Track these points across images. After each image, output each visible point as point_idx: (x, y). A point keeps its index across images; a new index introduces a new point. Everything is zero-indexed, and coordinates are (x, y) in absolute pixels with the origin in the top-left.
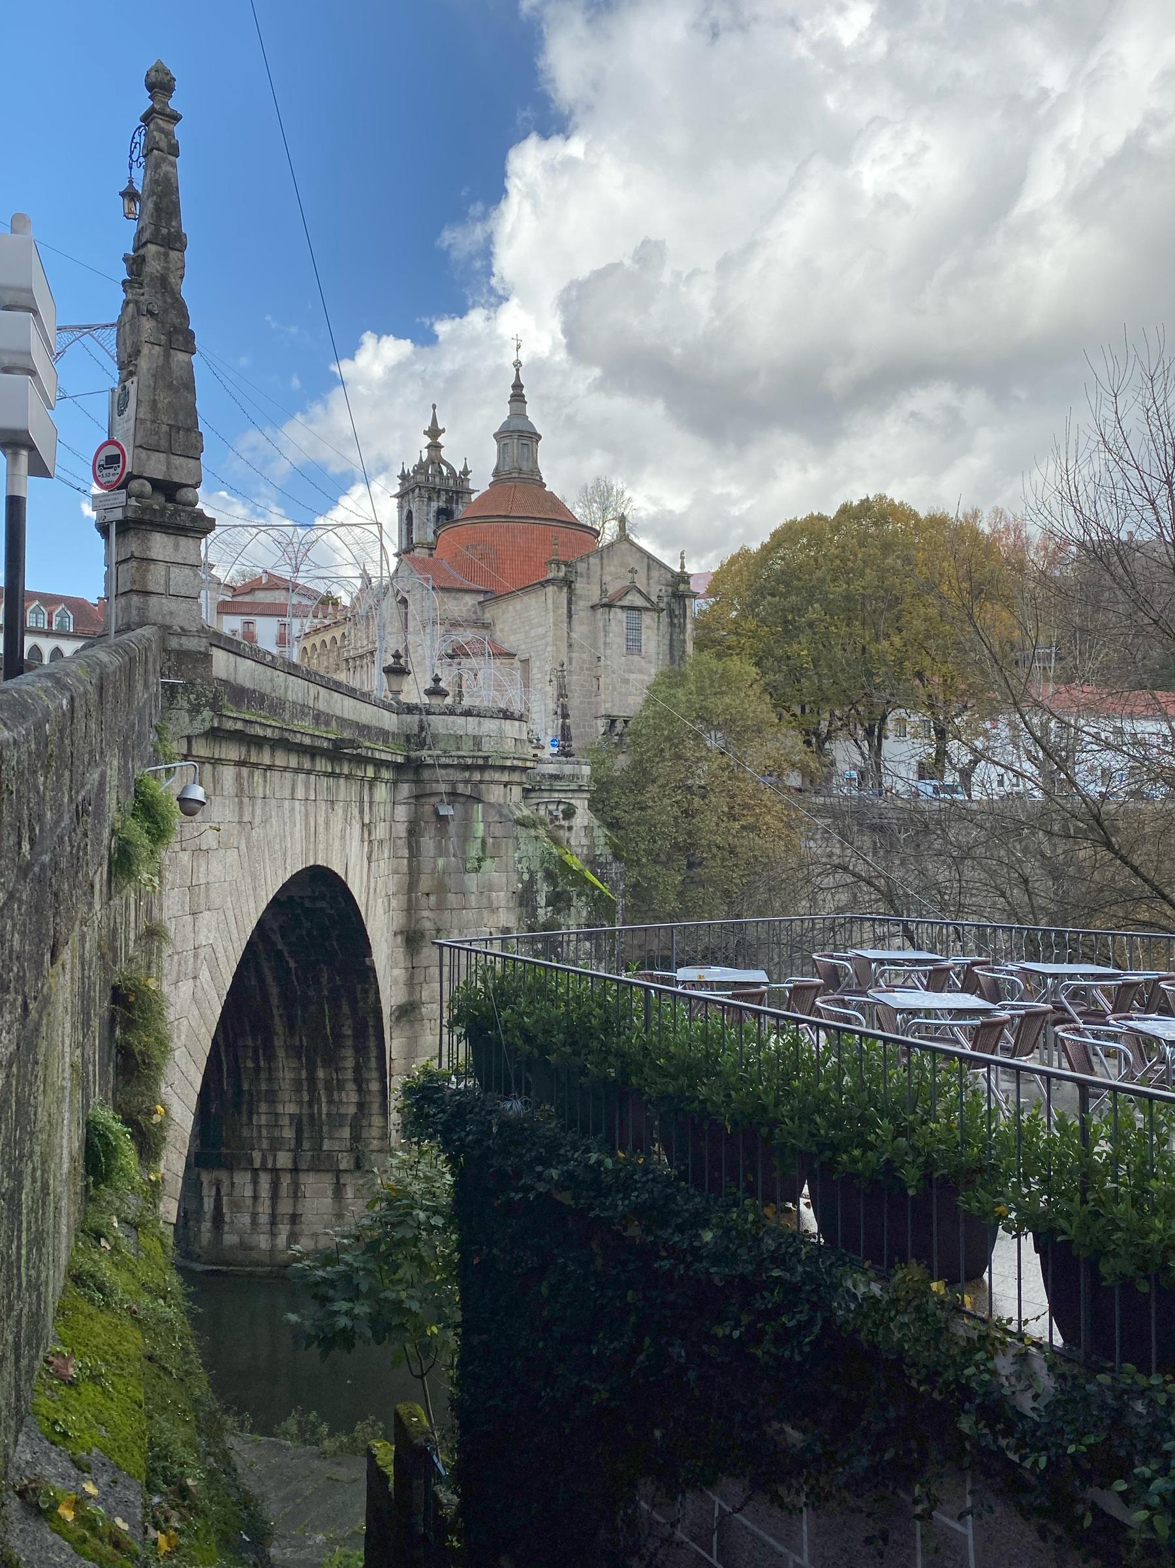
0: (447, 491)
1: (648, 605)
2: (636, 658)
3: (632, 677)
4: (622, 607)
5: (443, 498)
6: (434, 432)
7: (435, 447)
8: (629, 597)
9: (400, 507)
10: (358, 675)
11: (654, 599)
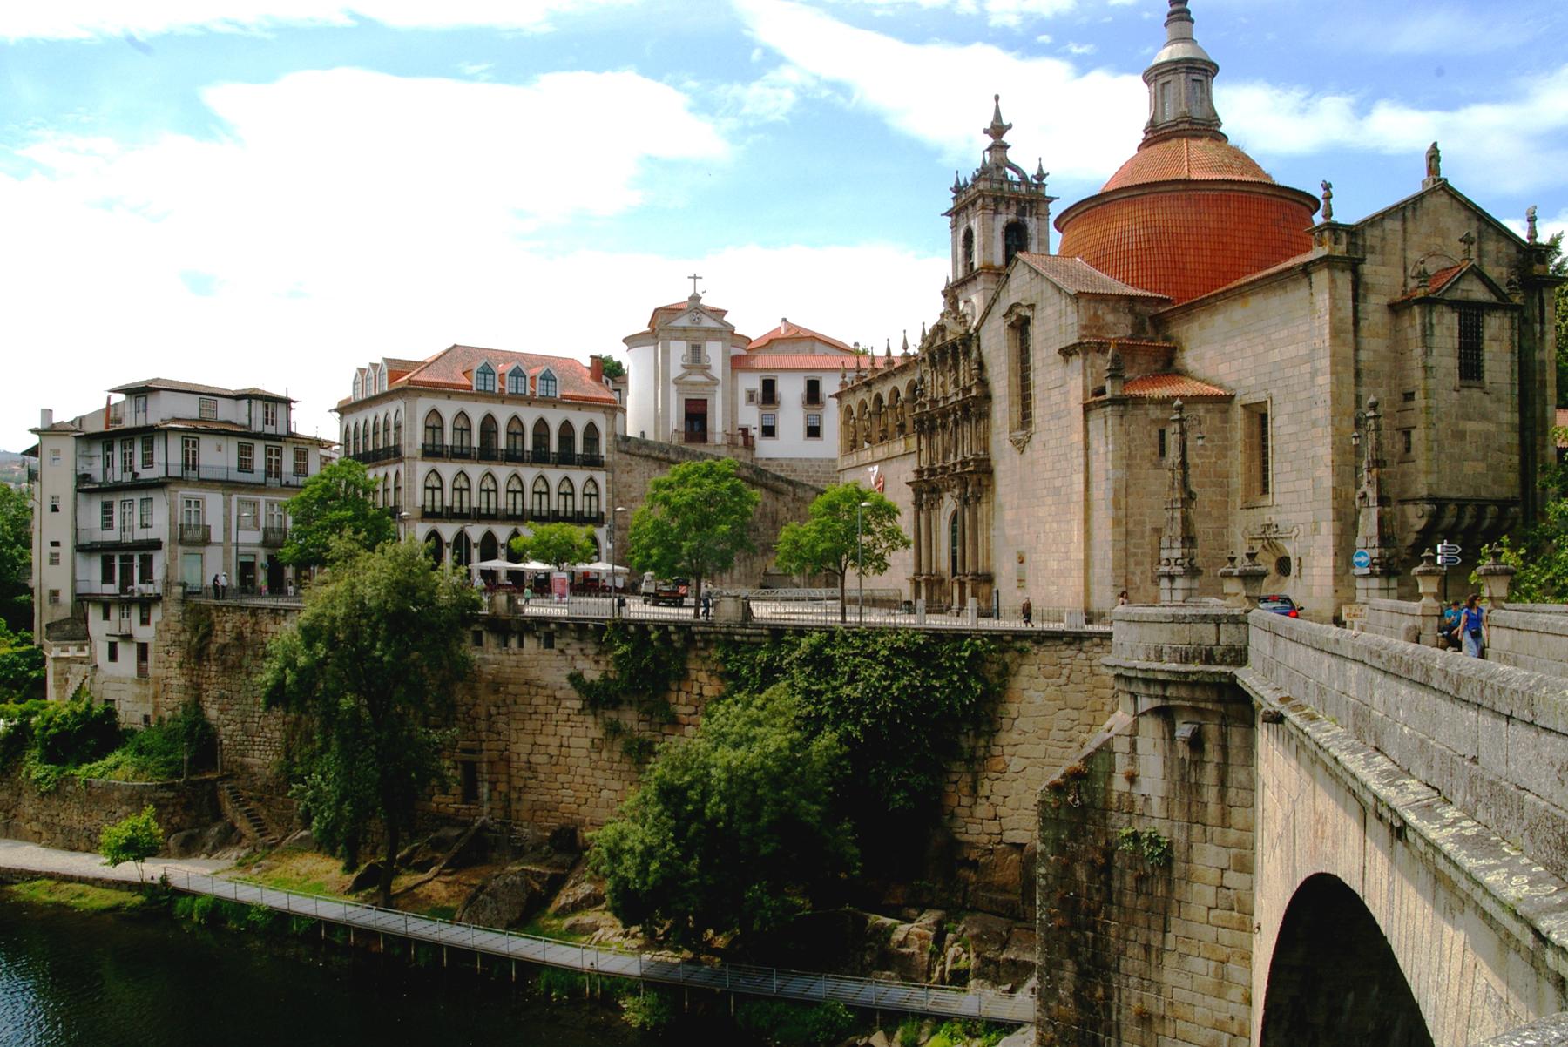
0: (1018, 202)
1: (1494, 299)
2: (1476, 394)
3: (1471, 426)
4: (1454, 305)
5: (1013, 209)
6: (998, 130)
7: (999, 147)
8: (1463, 286)
9: (954, 227)
10: (938, 440)
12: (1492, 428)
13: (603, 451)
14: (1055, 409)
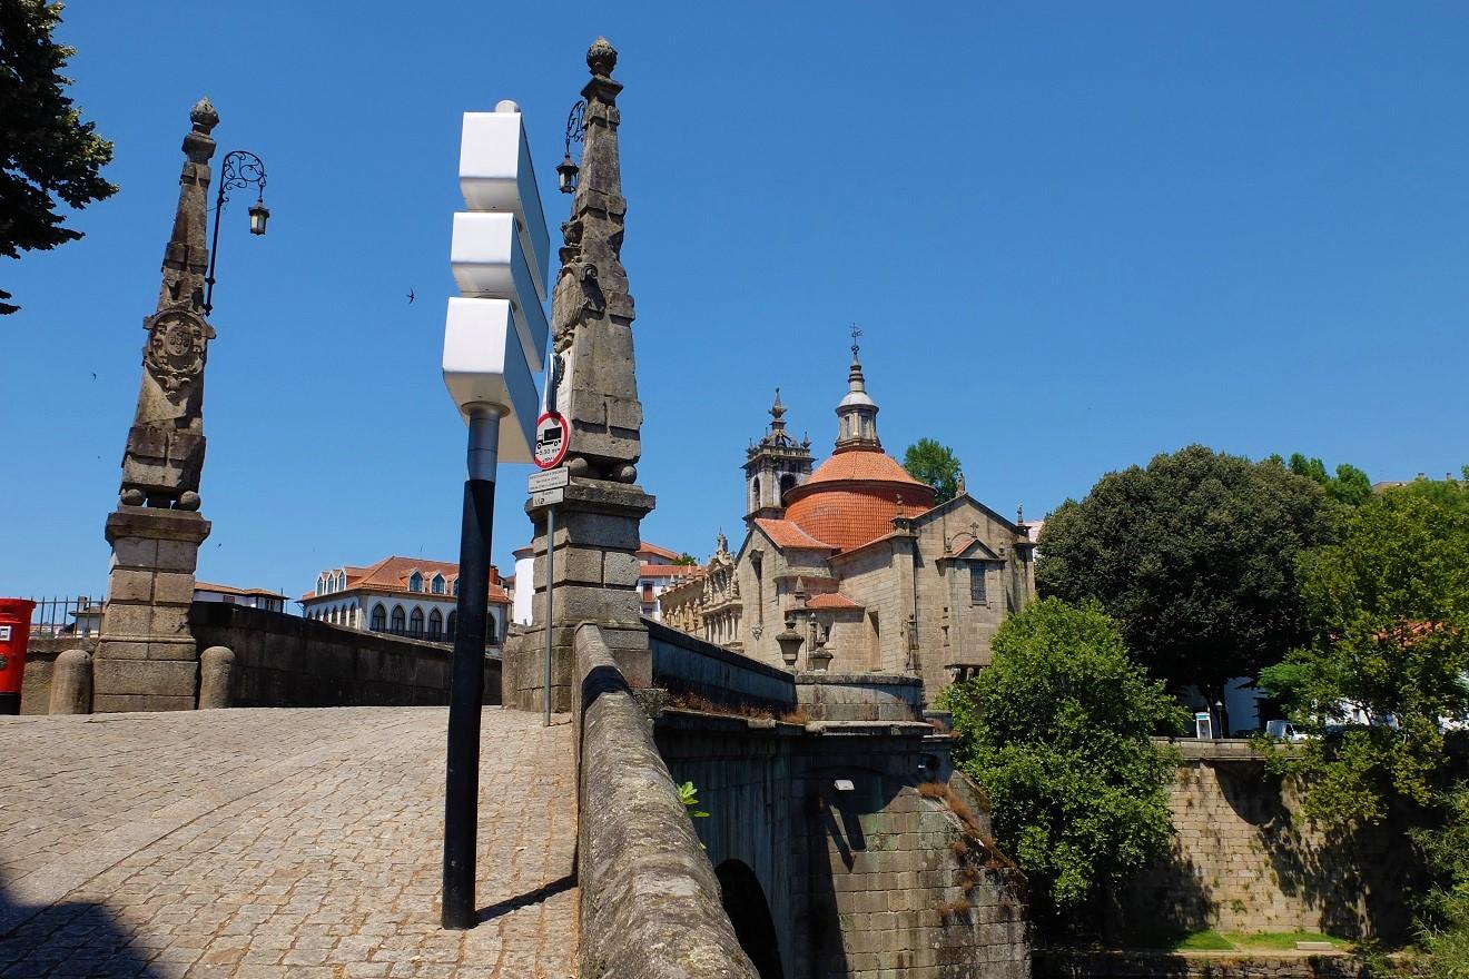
3: (980, 625)
5: (787, 466)
11: (996, 551)
12: (993, 626)
13: (497, 635)
14: (774, 613)
